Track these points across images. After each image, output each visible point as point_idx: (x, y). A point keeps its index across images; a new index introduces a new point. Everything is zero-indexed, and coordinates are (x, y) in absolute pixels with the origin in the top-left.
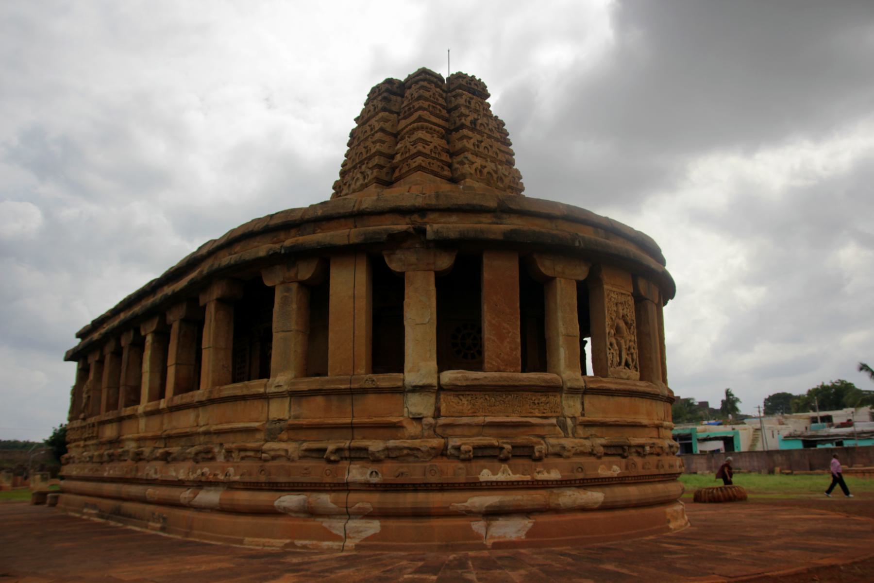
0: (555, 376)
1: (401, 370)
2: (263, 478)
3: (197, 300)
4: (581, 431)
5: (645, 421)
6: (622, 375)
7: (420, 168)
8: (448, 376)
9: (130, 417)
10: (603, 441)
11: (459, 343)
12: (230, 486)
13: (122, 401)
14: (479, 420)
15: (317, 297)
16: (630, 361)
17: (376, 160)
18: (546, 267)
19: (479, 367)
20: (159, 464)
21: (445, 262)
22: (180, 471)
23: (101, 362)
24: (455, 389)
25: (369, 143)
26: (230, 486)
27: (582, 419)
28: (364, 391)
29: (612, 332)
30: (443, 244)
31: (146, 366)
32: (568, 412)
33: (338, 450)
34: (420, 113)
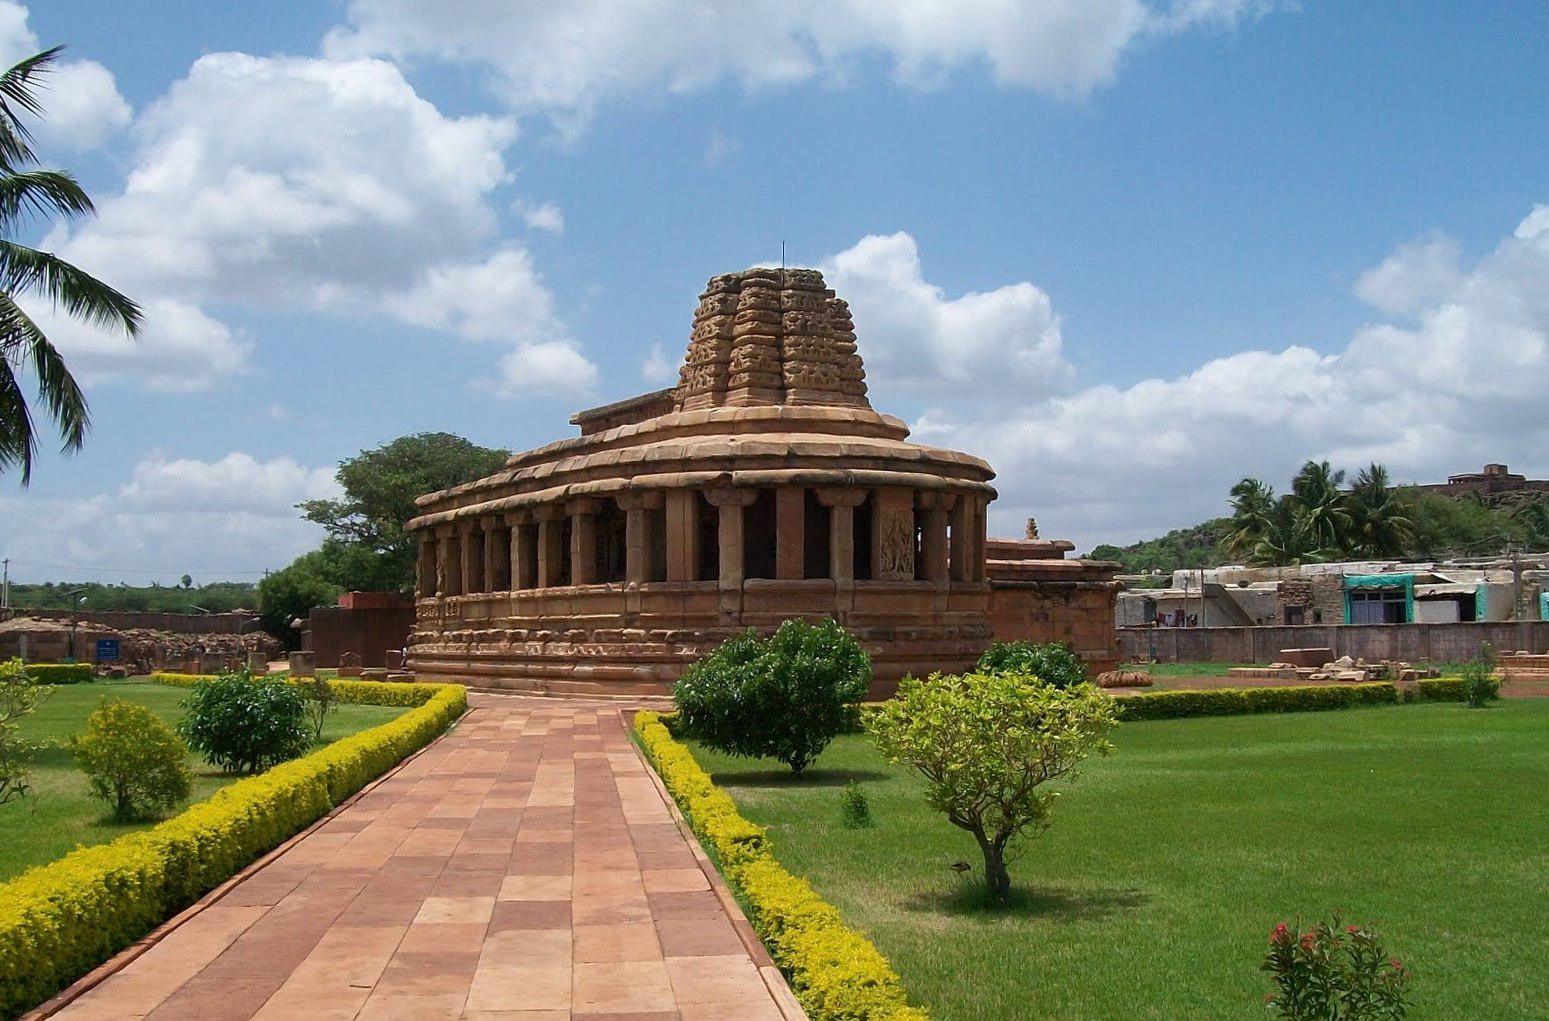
0: (830, 581)
1: (717, 579)
2: (624, 654)
3: (563, 505)
4: (850, 622)
5: (916, 614)
6: (894, 578)
7: (748, 384)
8: (749, 583)
9: (500, 600)
10: (869, 629)
11: (759, 559)
12: (600, 660)
13: (488, 583)
14: (767, 614)
15: (656, 520)
16: (904, 565)
17: (712, 368)
18: (826, 498)
19: (770, 574)
20: (538, 645)
21: (749, 498)
22: (561, 649)
23: (454, 541)
24: (756, 594)
25: (708, 345)
26: (600, 660)
27: (849, 613)
28: (691, 594)
29: (887, 543)
30: (744, 485)
31: (515, 556)
32: (840, 608)
33: (672, 635)
34: (749, 325)
